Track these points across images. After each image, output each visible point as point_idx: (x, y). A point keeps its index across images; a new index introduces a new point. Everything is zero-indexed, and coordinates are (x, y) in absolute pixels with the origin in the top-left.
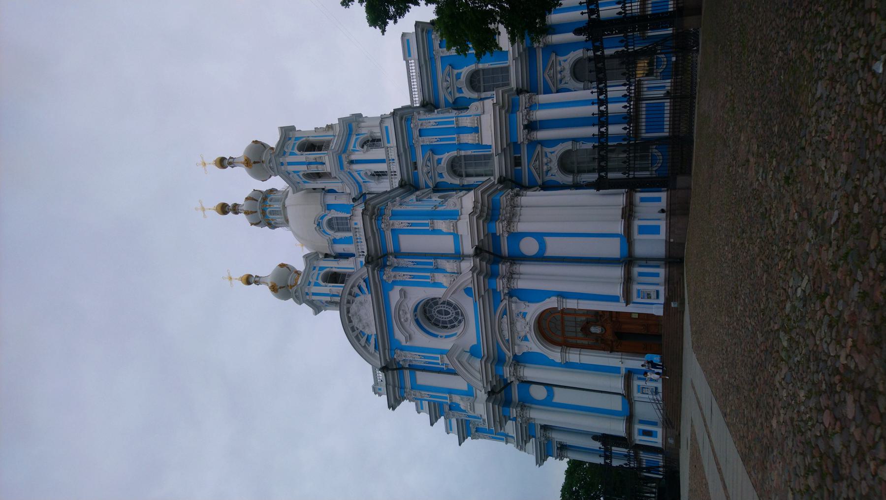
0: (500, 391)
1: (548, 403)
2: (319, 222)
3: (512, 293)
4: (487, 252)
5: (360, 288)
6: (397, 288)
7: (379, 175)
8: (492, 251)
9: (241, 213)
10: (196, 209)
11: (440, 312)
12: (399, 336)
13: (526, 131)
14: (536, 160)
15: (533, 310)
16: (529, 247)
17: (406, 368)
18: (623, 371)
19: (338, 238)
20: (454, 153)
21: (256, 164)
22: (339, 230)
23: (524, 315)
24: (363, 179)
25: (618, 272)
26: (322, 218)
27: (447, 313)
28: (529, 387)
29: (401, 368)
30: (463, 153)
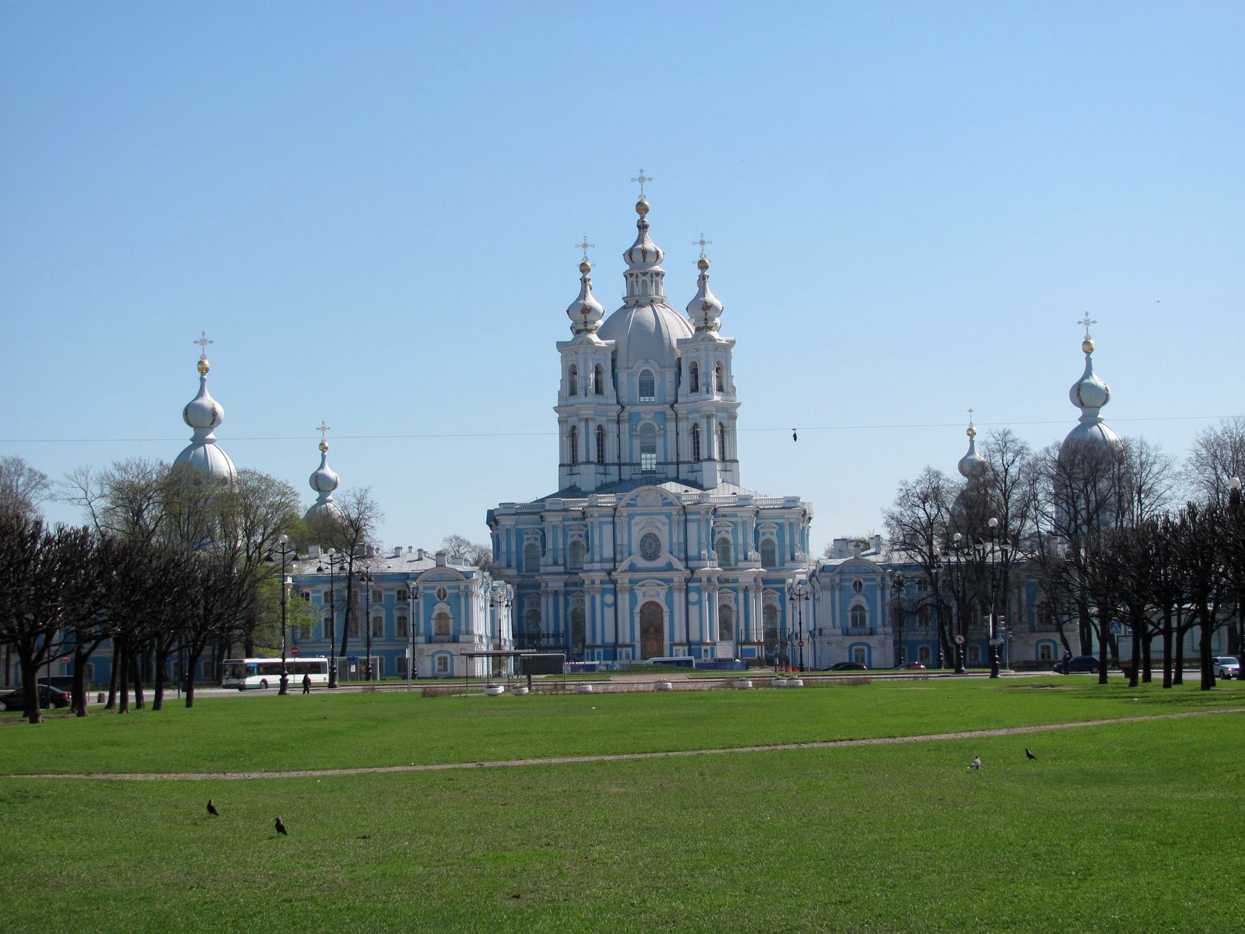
1: (603, 604)
3: (670, 591)
5: (666, 498)
6: (667, 521)
7: (694, 433)
9: (640, 232)
10: (642, 171)
11: (650, 544)
12: (638, 519)
13: (744, 587)
15: (661, 601)
16: (693, 597)
18: (633, 643)
20: (732, 541)
25: (684, 640)
29: (614, 516)
30: (732, 546)
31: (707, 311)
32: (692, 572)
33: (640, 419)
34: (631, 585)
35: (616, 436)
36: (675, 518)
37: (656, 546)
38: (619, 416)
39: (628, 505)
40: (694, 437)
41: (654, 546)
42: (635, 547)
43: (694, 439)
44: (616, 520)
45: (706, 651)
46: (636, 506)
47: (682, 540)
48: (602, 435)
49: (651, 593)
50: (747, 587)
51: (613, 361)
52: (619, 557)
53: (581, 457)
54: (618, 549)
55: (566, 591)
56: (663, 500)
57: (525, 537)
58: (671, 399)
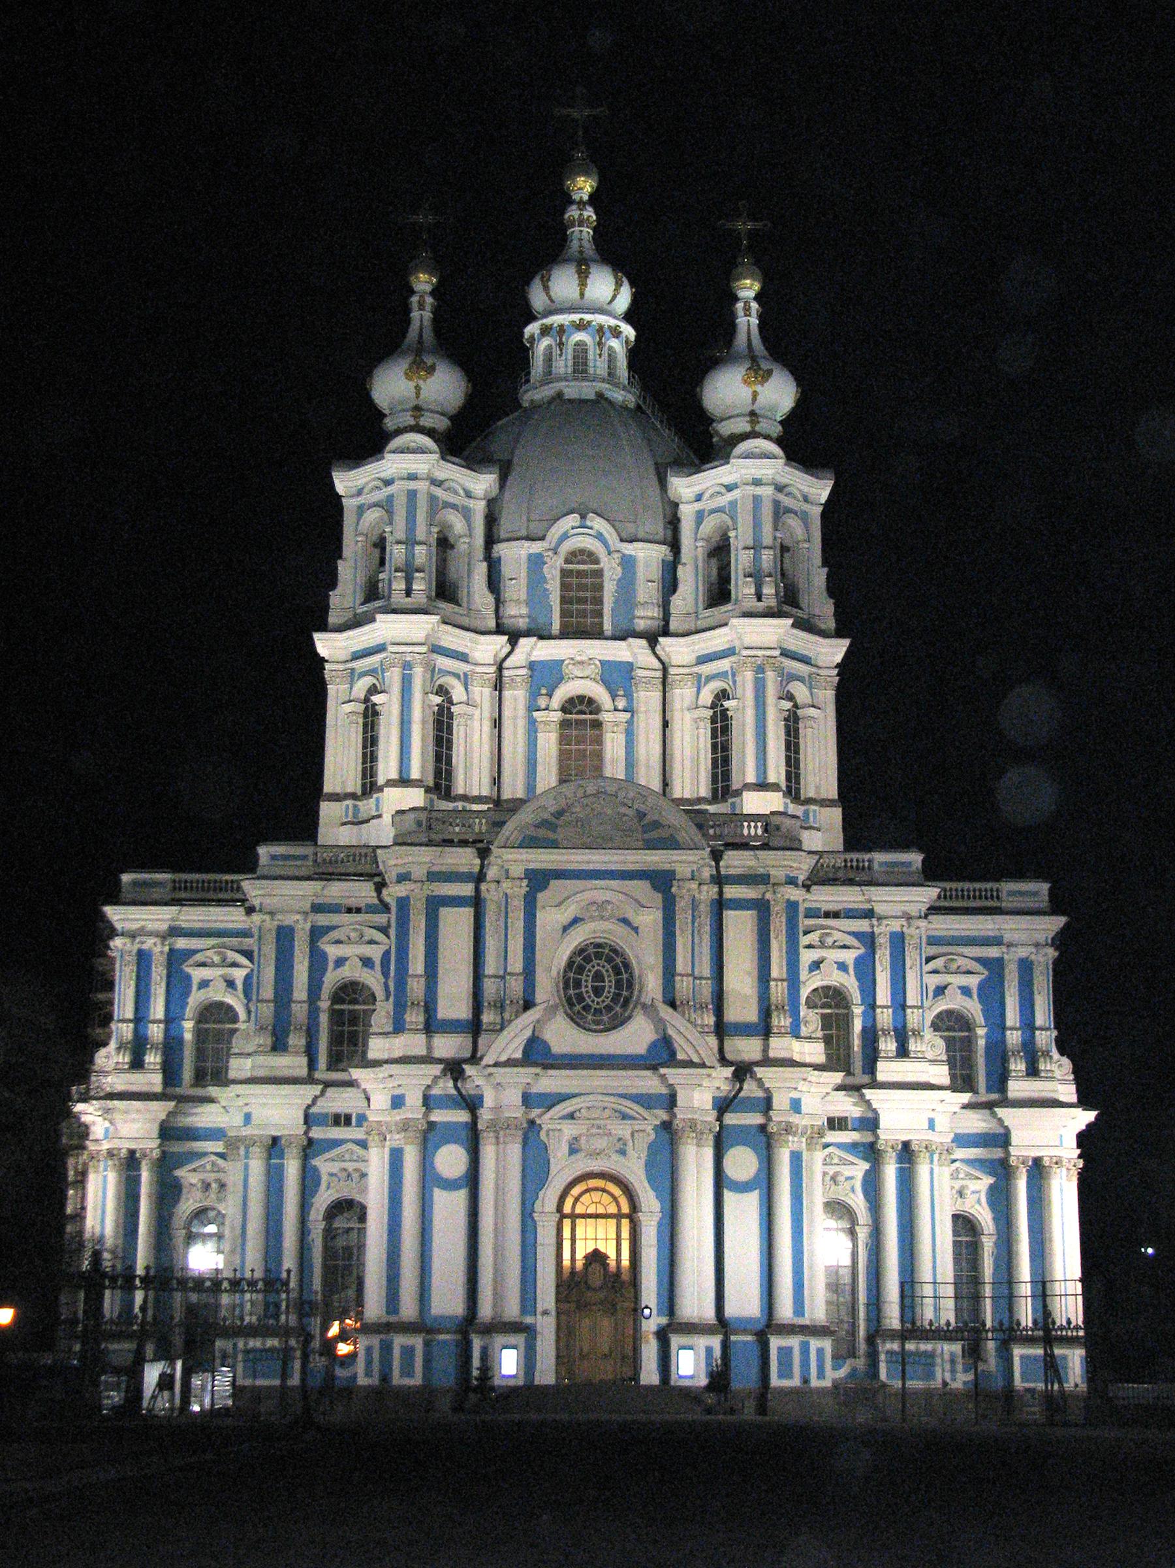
0: (456, 1087)
1: (429, 1179)
2: (591, 528)
4: (741, 1089)
7: (713, 720)
8: (740, 1095)
11: (598, 977)
14: (841, 1158)
17: (477, 890)
18: (529, 1320)
19: (546, 569)
20: (856, 996)
21: (750, 397)
22: (565, 573)
23: (623, 1152)
24: (710, 678)
25: (708, 1313)
26: (599, 537)
27: (598, 991)
28: (462, 1144)
31: (759, 388)
32: (742, 1071)
33: (560, 679)
34: (535, 1113)
35: (487, 726)
36: (684, 891)
37: (619, 984)
38: (500, 668)
39: (530, 842)
40: (714, 730)
41: (609, 983)
42: (546, 987)
43: (714, 736)
44: (484, 894)
45: (786, 1352)
46: (554, 845)
47: (705, 968)
48: (451, 716)
49: (601, 1143)
50: (906, 1145)
51: (491, 520)
52: (487, 1017)
53: (387, 768)
54: (490, 988)
55: (311, 1141)
56: (646, 829)
57: (198, 974)
58: (655, 625)
